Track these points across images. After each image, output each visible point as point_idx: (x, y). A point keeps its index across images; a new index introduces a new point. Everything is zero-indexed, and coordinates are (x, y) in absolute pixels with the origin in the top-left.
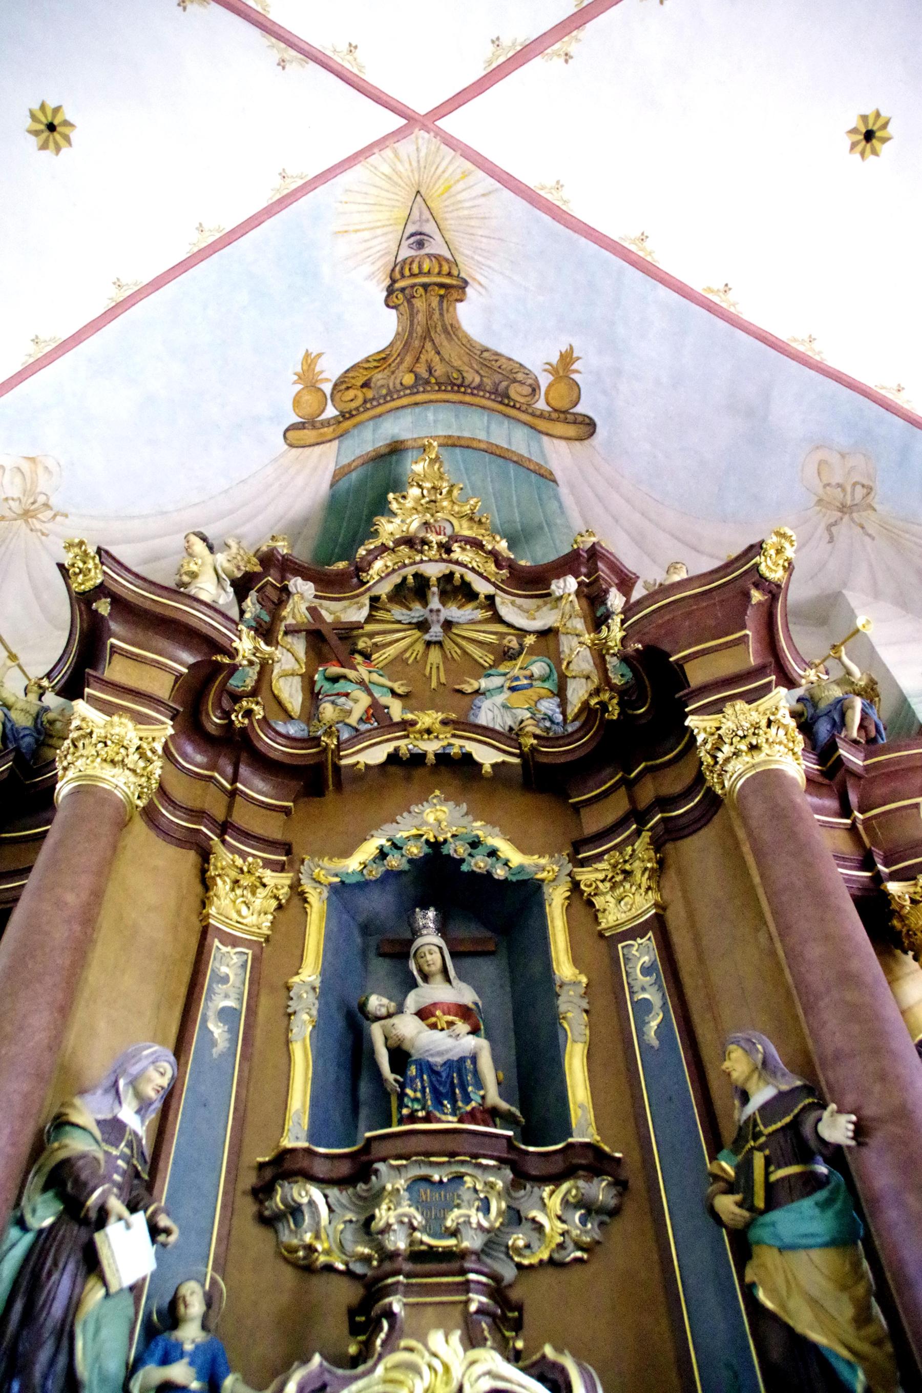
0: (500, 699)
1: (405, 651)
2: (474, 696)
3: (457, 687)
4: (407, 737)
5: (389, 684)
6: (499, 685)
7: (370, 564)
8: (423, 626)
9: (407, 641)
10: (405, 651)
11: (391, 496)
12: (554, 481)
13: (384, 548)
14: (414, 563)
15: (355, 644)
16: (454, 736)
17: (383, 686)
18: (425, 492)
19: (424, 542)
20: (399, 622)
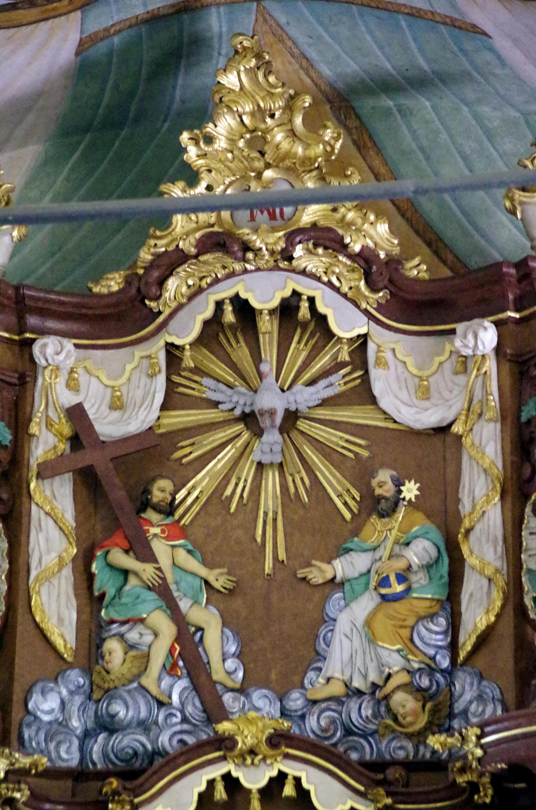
0: (365, 604)
1: (226, 480)
2: (327, 590)
3: (301, 574)
4: (224, 758)
5: (203, 571)
6: (364, 570)
7: (161, 283)
8: (250, 419)
9: (228, 453)
10: (226, 480)
11: (185, 136)
12: (485, 34)
13: (179, 258)
14: (232, 274)
15: (147, 491)
16: (287, 756)
17: (194, 574)
18: (247, 120)
19: (246, 247)
20: (216, 404)
